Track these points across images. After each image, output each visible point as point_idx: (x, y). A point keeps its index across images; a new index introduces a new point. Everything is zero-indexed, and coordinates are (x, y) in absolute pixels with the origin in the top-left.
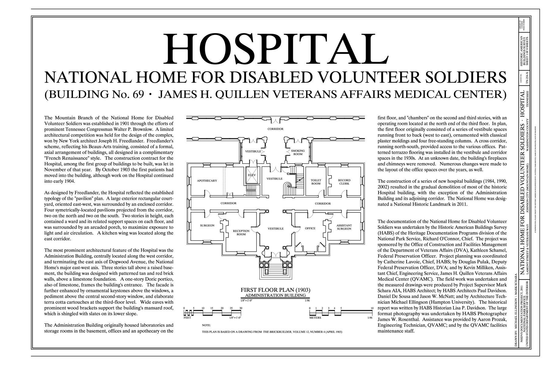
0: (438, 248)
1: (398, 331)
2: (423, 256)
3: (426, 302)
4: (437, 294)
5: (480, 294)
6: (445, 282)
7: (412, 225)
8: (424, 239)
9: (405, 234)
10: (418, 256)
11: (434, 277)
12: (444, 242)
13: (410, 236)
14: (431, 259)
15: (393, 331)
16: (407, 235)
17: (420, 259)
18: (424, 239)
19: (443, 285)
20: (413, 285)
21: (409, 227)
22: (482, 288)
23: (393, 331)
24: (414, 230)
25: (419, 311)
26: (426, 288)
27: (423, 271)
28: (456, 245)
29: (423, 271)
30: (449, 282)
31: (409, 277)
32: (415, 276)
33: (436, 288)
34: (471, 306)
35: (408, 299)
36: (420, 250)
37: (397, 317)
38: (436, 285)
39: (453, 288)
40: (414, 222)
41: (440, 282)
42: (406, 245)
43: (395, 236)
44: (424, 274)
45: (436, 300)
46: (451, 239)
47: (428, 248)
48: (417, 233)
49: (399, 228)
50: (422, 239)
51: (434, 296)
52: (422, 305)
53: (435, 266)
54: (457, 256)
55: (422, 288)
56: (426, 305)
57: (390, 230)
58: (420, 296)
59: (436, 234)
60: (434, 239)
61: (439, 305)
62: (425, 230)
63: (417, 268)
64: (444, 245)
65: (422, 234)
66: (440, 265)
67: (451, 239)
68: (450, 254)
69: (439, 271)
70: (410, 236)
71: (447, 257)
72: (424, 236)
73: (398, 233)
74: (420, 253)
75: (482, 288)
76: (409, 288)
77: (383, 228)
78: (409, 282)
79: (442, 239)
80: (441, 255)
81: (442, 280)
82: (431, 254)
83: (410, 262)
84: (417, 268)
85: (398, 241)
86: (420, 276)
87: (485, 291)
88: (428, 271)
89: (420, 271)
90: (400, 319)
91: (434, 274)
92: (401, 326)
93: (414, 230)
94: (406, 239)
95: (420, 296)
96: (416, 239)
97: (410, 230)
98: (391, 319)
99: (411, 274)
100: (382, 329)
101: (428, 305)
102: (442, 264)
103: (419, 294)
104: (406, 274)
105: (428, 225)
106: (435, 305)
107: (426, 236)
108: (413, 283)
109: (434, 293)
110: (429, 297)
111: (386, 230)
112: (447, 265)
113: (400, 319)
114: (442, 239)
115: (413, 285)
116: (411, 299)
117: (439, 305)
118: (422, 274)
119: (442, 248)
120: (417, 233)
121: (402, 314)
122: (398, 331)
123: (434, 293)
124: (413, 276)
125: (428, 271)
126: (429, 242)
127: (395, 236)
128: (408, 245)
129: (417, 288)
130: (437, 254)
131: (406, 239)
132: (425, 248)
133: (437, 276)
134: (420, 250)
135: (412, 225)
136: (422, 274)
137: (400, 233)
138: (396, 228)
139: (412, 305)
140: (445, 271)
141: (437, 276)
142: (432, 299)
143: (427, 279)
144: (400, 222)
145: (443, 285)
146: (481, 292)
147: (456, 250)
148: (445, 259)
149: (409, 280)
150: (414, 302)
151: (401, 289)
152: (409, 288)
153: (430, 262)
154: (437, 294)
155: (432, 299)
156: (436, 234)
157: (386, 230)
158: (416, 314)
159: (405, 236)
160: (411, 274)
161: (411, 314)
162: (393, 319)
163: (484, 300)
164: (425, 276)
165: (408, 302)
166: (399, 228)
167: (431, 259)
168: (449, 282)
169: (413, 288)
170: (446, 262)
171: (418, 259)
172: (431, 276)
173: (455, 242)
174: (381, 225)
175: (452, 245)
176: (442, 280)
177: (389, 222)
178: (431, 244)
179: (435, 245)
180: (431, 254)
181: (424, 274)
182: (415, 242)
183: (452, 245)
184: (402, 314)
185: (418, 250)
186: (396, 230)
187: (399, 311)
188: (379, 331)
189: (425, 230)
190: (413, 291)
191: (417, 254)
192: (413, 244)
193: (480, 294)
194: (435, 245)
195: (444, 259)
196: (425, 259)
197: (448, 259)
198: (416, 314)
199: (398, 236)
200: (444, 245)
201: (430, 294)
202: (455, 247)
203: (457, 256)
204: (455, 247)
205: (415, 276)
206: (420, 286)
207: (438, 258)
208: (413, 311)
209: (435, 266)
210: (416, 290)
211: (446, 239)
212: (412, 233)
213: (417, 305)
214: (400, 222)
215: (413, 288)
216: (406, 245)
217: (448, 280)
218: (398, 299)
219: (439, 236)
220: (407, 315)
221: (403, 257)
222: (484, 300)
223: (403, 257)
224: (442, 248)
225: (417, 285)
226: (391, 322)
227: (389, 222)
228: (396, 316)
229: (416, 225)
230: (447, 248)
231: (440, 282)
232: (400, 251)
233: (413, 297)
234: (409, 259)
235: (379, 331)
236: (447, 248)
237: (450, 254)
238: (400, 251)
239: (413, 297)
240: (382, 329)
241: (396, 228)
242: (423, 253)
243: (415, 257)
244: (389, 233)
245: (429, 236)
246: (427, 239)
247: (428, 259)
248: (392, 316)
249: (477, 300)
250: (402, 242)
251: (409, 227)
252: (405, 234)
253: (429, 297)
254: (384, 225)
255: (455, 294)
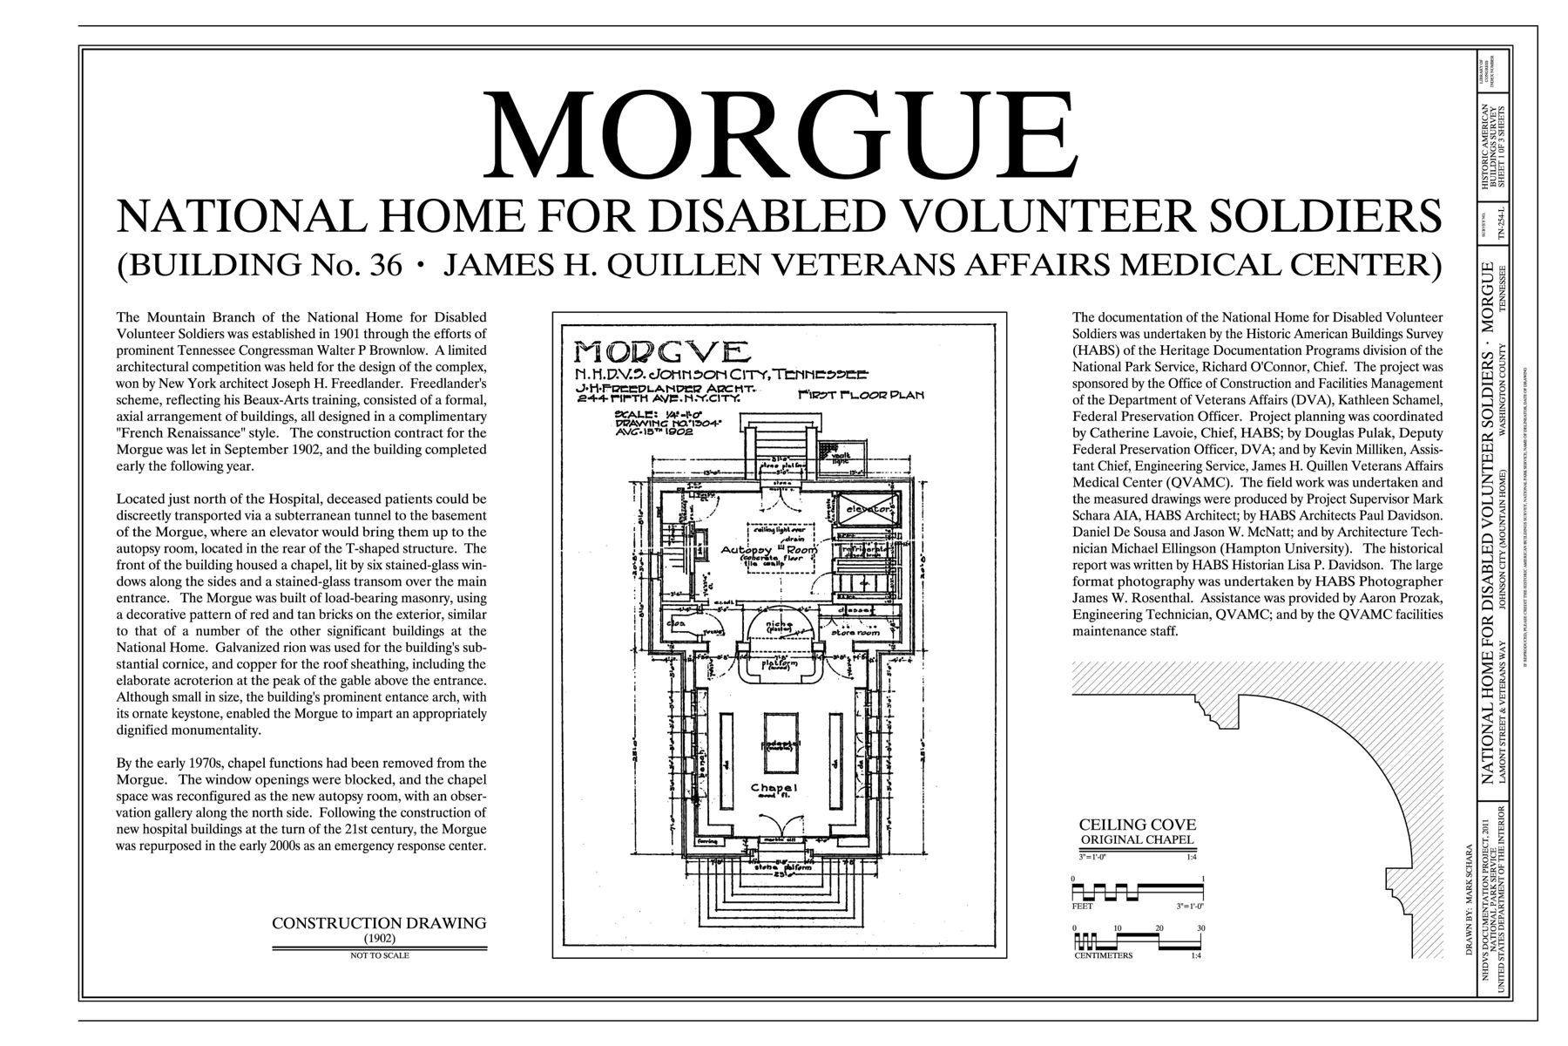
0: (1247, 393)
1: (1133, 632)
2: (1203, 416)
3: (1212, 549)
4: (1244, 525)
5: (1366, 524)
6: (1266, 491)
7: (1170, 327)
8: (1206, 367)
9: (1151, 352)
10: (1189, 417)
11: (1235, 477)
12: (1262, 376)
13: (1167, 360)
14: (1226, 426)
15: (1117, 632)
16: (1158, 357)
17: (1195, 426)
18: (1206, 367)
19: (1259, 499)
20: (1174, 500)
21: (1164, 335)
22: (1372, 509)
23: (1117, 632)
24: (1176, 343)
25: (1191, 574)
26: (1211, 507)
27: (1202, 459)
28: (1298, 385)
29: (1202, 459)
30: (1279, 492)
31: (1162, 475)
32: (1181, 474)
33: (1241, 508)
34: (1341, 560)
35: (1160, 540)
36: (1194, 400)
37: (1128, 591)
38: (1240, 500)
39: (1288, 507)
40: (1178, 318)
41: (1252, 492)
42: (1154, 384)
43: (1123, 358)
44: (1204, 467)
45: (1241, 541)
46: (1281, 368)
47: (1218, 392)
48: (1186, 351)
49: (1135, 335)
50: (1199, 365)
51: (1234, 532)
52: (1198, 556)
53: (1236, 444)
54: (1301, 417)
55: (1201, 508)
56: (1211, 557)
57: (1107, 342)
58: (1193, 532)
59: (1242, 352)
60: (1233, 368)
61: (1249, 558)
62: (1208, 343)
63: (1186, 450)
64: (1263, 385)
65: (1200, 353)
66: (1250, 441)
67: (1281, 368)
68: (1279, 409)
69: (1248, 460)
70: (1167, 360)
71: (1273, 418)
72: (1205, 359)
73: (1131, 351)
74: (1194, 408)
75: (1372, 509)
76: (1164, 507)
77: (1088, 335)
78: (1163, 491)
79: (1256, 366)
80: (1253, 415)
81: (1258, 484)
82: (1226, 409)
83: (1166, 434)
84: (1186, 450)
85: (1131, 374)
86: (1193, 474)
87: (1379, 517)
88: (1217, 459)
89: (1194, 458)
90: (1136, 598)
91: (1233, 468)
92: (1139, 618)
93: (1176, 343)
94: (1153, 367)
95: (1193, 532)
96: (1183, 369)
97: (1165, 342)
98: (1110, 598)
99: (1167, 467)
100: (1085, 624)
101: (1218, 556)
102: (1257, 440)
103: (1192, 524)
104: (1153, 468)
105: (1216, 327)
106: (1238, 557)
107: (1210, 358)
108: (1174, 492)
109: (1233, 523)
110: (1220, 533)
111: (1097, 342)
112: (1273, 442)
113: (1136, 598)
114: (1256, 366)
115: (1174, 500)
116: (1168, 539)
117: (1249, 558)
118: (1198, 469)
119: (1258, 392)
120: (1186, 351)
121: (1143, 582)
122: (1133, 632)
123: (1233, 523)
124: (1174, 474)
125: (1217, 459)
126: (1220, 375)
127: (1123, 358)
128: (1160, 385)
129: (1185, 509)
130: (1243, 411)
131: (1153, 367)
132: (1210, 393)
133: (1244, 474)
134: (1194, 400)
135: (1170, 327)
136: (1198, 469)
137: (1136, 351)
138: (1124, 335)
139: (1171, 558)
140: (1264, 459)
141: (1244, 474)
142: (1229, 538)
143: (1214, 482)
144: (1135, 319)
145: (1259, 499)
146: (1370, 518)
147: (1298, 400)
148: (1267, 424)
149: (1163, 484)
150: (1177, 549)
151: (1140, 510)
152: (1164, 507)
153: (1223, 435)
154: (1244, 525)
155: (1229, 538)
156: (1242, 352)
157: (1097, 342)
158: (1183, 582)
159: (1151, 360)
160: (1167, 467)
161: (1170, 583)
162: (1118, 598)
163: (1379, 541)
164: (1210, 475)
165: (1160, 548)
166: (1135, 335)
167: (1226, 426)
168: (1279, 492)
169: (1173, 507)
170: (1269, 433)
171: (1189, 426)
172: (1224, 473)
173: (1293, 377)
174: (1083, 327)
175: (1287, 384)
176: (1258, 484)
177: (1104, 318)
178: (1226, 383)
179: (1239, 384)
180: (1226, 409)
181: (1204, 467)
182: (1179, 375)
183: (1287, 384)
184: (1143, 582)
185: (1188, 400)
186: (1125, 343)
187: (1134, 574)
188: (1076, 632)
189: (1208, 343)
190: (1172, 515)
191: (1184, 410)
192: (1173, 383)
193: (1366, 524)
194: (1239, 384)
195: (1262, 425)
196: (1208, 424)
197: (1275, 424)
198: (1183, 582)
199: (1130, 358)
200: (1263, 385)
201: (1224, 525)
202: (1294, 391)
203: (1301, 417)
204: (1294, 391)
205: (1181, 474)
206: (1193, 501)
207: (1247, 424)
208: (1175, 574)
209: (1236, 444)
210: (1184, 515)
211: (1269, 367)
212: (1170, 351)
213: (1185, 558)
214: (1135, 319)
215: (1173, 507)
216: (1154, 384)
217: (1275, 484)
218: (1130, 541)
219: (1250, 359)
220: (1156, 584)
221: (1146, 418)
222: (1379, 541)
223: (1146, 418)
224: (1258, 392)
225: (1183, 500)
226: (1111, 606)
227: (1104, 318)
228: (1124, 589)
229: (1182, 327)
230: (1271, 393)
231: (1252, 492)
232: (1137, 402)
233: (1173, 534)
234: (1163, 426)
235: (1076, 632)
236: (1271, 393)
237: (1279, 409)
238: (1137, 402)
239: (1173, 534)
240: (1085, 624)
241: (1124, 335)
242: (1204, 407)
243: (1179, 418)
244: (1104, 350)
245: (1218, 360)
246: (1215, 369)
247: (1217, 425)
248: (1115, 589)
249: (1357, 544)
250: (1143, 376)
251: (1164, 335)
252: (1151, 352)
253: (1220, 533)
254: (1092, 326)
255: (1296, 525)
